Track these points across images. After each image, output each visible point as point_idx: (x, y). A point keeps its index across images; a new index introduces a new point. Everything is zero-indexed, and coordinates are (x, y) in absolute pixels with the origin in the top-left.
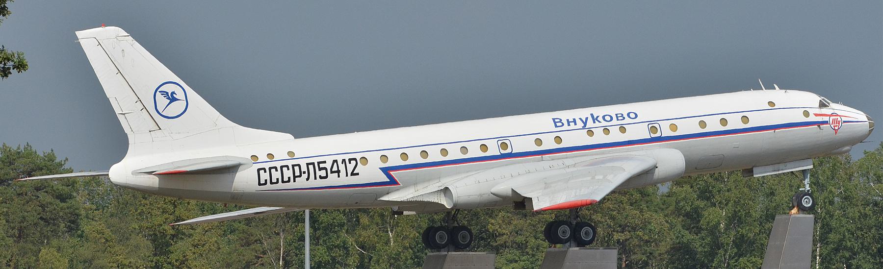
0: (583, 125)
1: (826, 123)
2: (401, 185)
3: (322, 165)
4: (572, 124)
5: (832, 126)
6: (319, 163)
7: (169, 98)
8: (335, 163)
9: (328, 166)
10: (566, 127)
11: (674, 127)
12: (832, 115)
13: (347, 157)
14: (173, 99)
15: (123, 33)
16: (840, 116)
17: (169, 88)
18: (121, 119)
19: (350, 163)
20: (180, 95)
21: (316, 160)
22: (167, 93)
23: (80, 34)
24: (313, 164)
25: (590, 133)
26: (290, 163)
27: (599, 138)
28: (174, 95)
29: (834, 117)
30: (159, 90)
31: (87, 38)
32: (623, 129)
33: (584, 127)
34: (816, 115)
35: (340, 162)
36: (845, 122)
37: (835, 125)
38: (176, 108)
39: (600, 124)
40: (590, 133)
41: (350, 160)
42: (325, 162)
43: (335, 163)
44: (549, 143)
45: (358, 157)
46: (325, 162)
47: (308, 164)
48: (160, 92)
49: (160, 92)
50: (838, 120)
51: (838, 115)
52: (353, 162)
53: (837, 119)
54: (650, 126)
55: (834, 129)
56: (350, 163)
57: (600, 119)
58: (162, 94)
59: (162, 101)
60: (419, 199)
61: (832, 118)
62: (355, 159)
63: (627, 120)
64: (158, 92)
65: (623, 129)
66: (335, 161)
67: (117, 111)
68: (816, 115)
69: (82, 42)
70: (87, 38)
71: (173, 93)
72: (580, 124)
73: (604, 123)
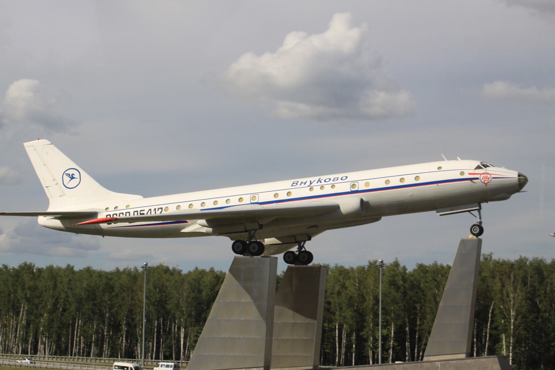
0: (309, 184)
1: (477, 179)
2: (190, 223)
3: (142, 212)
4: (303, 184)
5: (482, 181)
6: (141, 211)
7: (70, 177)
8: (150, 211)
9: (145, 212)
10: (298, 186)
11: (367, 184)
12: (483, 174)
13: (157, 207)
14: (72, 178)
15: (48, 142)
16: (490, 174)
17: (71, 172)
18: (46, 189)
19: (158, 210)
20: (77, 175)
21: (139, 210)
22: (69, 175)
23: (26, 144)
24: (137, 211)
25: (311, 189)
26: (124, 212)
27: (317, 191)
28: (73, 176)
29: (484, 175)
30: (66, 172)
31: (30, 147)
32: (333, 186)
33: (309, 186)
34: (470, 174)
35: (152, 210)
36: (493, 178)
37: (485, 180)
38: (74, 182)
39: (321, 184)
40: (311, 189)
41: (158, 209)
42: (144, 210)
43: (150, 211)
44: (283, 196)
45: (164, 207)
46: (144, 210)
47: (134, 212)
48: (66, 174)
49: (66, 174)
50: (488, 177)
51: (488, 174)
52: (160, 210)
53: (487, 176)
54: (352, 184)
55: (484, 183)
56: (158, 210)
57: (323, 181)
58: (67, 175)
59: (67, 179)
60: (195, 231)
61: (482, 175)
62: (162, 208)
63: (340, 180)
64: (64, 174)
65: (333, 186)
66: (150, 210)
67: (44, 185)
68: (470, 174)
69: (27, 149)
70: (30, 147)
71: (73, 174)
72: (308, 183)
73: (323, 183)
